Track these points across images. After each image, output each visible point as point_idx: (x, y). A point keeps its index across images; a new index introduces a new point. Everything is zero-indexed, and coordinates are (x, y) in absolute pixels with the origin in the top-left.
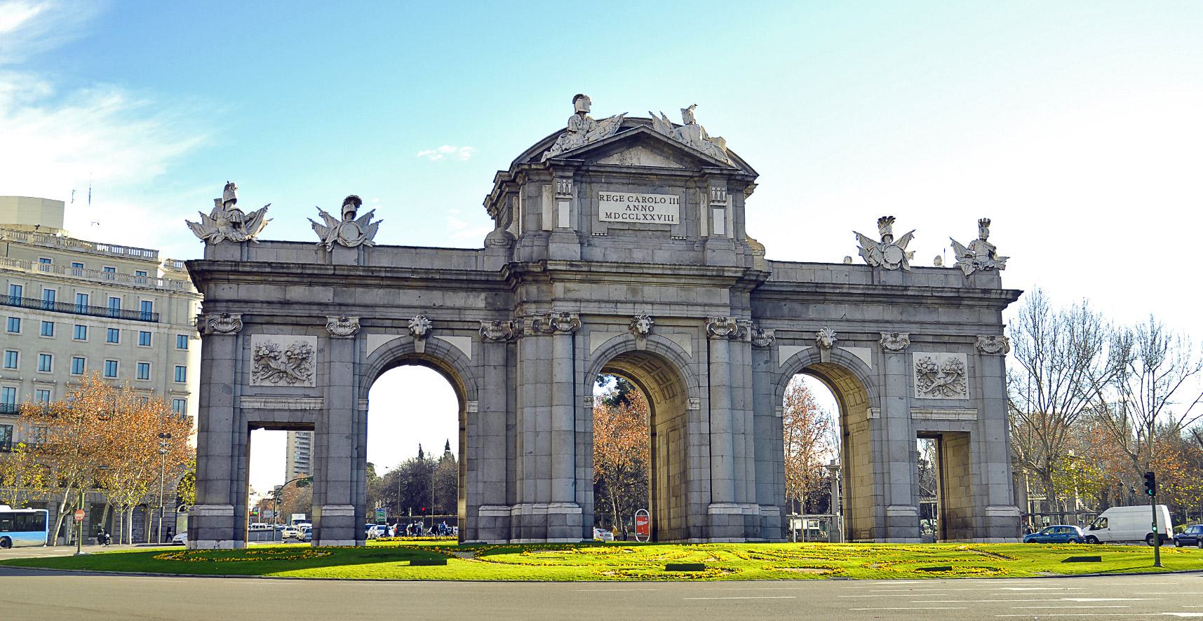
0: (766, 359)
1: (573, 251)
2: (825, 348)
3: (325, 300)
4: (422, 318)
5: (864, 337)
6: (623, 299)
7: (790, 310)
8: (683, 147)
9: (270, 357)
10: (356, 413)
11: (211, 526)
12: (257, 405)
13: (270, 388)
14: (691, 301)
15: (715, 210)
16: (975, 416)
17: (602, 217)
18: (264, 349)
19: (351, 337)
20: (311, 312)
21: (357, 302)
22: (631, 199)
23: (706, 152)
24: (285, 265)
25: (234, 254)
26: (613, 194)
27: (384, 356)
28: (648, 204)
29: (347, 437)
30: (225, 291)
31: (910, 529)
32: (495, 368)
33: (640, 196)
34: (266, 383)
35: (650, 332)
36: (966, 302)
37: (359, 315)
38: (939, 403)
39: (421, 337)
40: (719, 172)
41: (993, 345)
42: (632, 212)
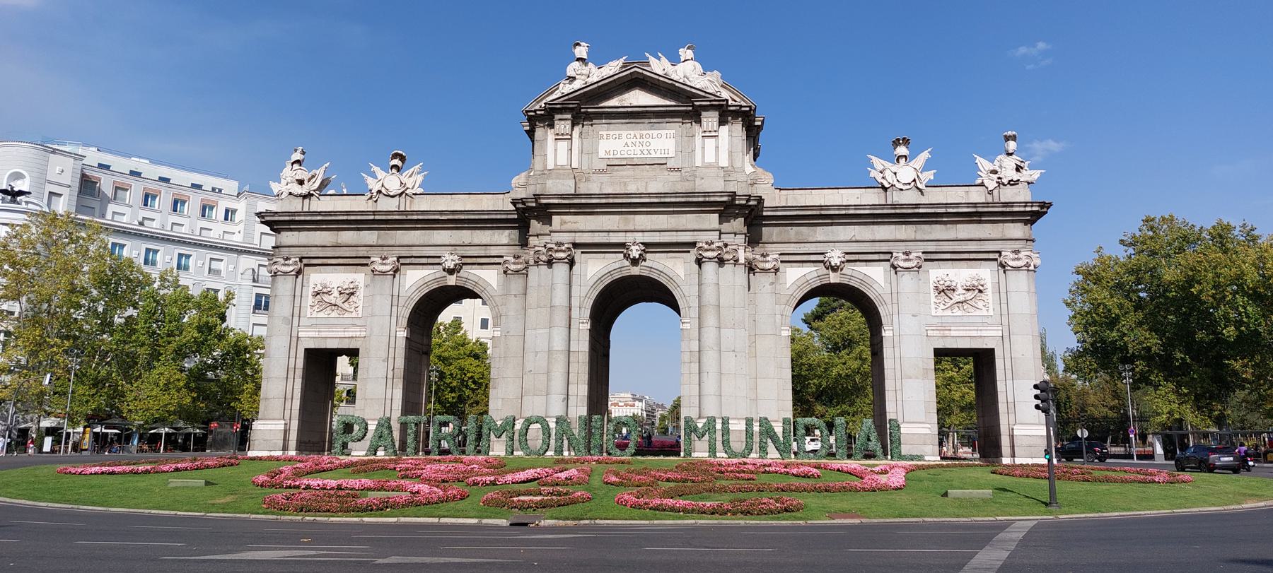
0: (771, 281)
1: (567, 187)
2: (835, 269)
3: (371, 243)
4: (452, 254)
5: (876, 257)
6: (615, 228)
7: (797, 233)
8: (674, 83)
9: (323, 293)
10: (393, 339)
11: (265, 438)
14: (681, 228)
15: (707, 140)
16: (1001, 332)
17: (602, 155)
18: (319, 285)
19: (391, 273)
21: (398, 244)
22: (629, 136)
23: (697, 87)
25: (296, 205)
26: (611, 133)
27: (420, 289)
28: (645, 140)
29: (384, 361)
30: (289, 237)
31: (923, 447)
32: (516, 297)
33: (638, 133)
35: (642, 258)
38: (958, 320)
39: (451, 272)
40: (708, 103)
41: (1018, 259)
42: (630, 148)
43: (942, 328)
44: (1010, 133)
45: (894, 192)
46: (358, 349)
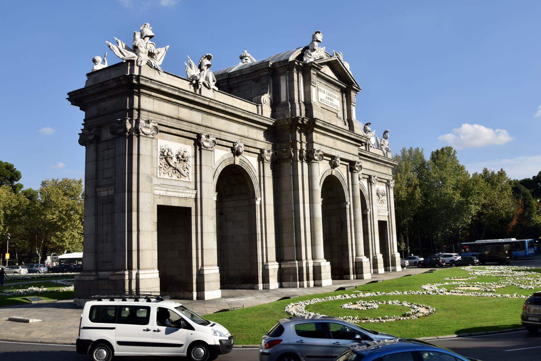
3: (198, 122)
12: (162, 193)
18: (167, 151)
20: (192, 128)
21: (213, 126)
24: (187, 93)
26: (322, 89)
28: (331, 97)
32: (268, 178)
34: (166, 176)
37: (214, 135)
40: (355, 88)
43: (378, 210)
45: (370, 148)
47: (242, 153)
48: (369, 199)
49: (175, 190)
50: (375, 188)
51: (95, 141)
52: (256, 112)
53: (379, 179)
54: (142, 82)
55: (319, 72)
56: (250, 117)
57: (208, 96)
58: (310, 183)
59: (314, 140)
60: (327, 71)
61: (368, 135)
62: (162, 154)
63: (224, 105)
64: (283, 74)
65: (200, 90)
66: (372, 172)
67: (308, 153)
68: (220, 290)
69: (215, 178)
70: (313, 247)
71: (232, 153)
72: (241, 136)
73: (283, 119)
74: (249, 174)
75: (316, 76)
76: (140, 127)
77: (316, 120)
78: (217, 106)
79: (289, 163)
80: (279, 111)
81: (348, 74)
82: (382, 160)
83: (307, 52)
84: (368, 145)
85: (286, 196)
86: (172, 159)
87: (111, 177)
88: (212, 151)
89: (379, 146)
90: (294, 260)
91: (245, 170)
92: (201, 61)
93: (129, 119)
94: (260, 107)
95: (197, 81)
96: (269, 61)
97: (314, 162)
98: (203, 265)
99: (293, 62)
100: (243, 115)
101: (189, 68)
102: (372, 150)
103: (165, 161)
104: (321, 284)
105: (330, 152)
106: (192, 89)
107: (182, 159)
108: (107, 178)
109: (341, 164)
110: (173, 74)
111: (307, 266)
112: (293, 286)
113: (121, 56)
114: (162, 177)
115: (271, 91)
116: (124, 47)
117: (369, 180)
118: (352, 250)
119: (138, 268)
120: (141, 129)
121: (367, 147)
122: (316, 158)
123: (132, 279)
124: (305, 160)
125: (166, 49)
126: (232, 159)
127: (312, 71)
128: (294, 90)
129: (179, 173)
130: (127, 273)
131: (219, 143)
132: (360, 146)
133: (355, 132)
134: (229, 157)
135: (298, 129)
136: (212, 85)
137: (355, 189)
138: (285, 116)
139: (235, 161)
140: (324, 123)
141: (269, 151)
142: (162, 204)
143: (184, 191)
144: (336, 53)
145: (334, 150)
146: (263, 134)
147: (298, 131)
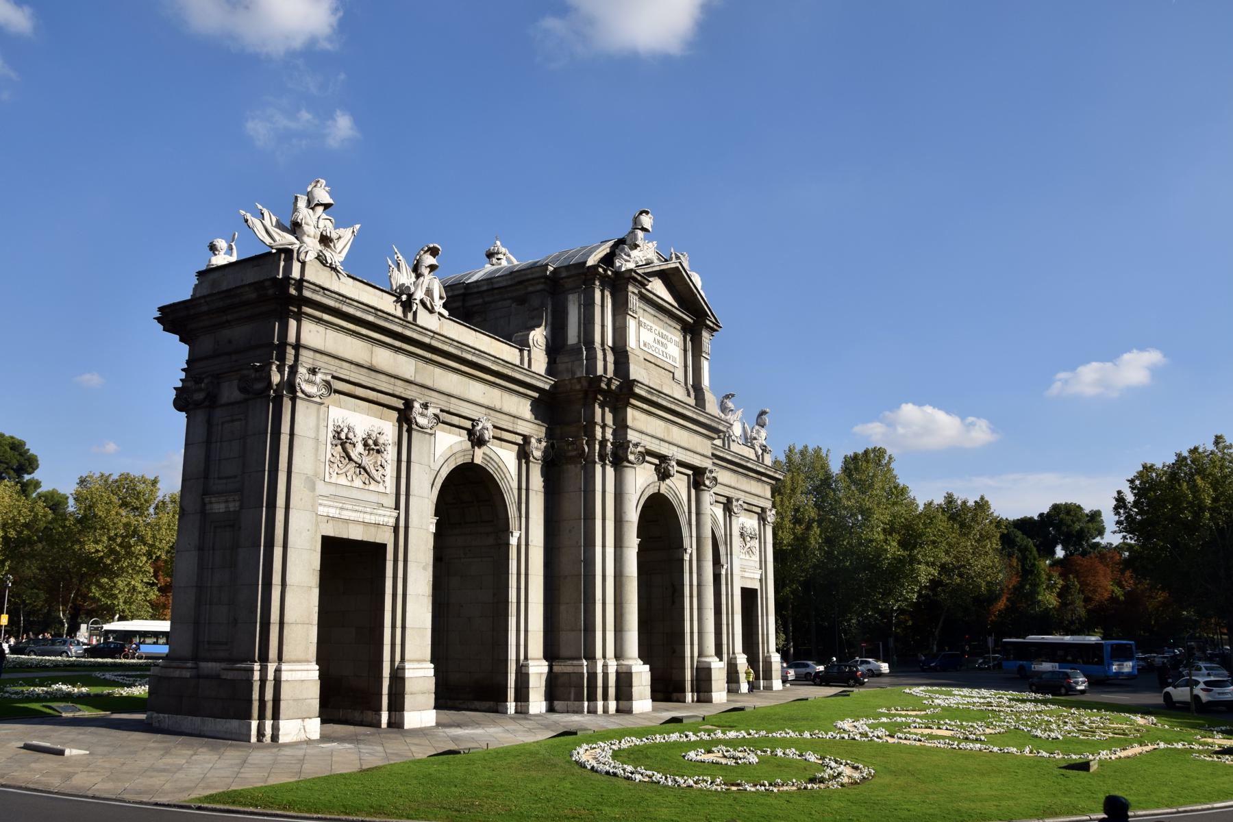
3: (407, 376)
12: (333, 512)
13: (344, 488)
18: (346, 430)
20: (396, 388)
21: (436, 387)
24: (391, 318)
26: (648, 323)
28: (663, 340)
36: (763, 478)
40: (711, 324)
44: (768, 410)
45: (731, 443)
46: (386, 545)
47: (488, 442)
48: (726, 544)
49: (357, 508)
50: (737, 524)
51: (207, 403)
52: (518, 363)
53: (745, 506)
54: (307, 293)
55: (643, 291)
56: (508, 371)
57: (429, 327)
58: (618, 506)
59: (629, 423)
60: (658, 288)
61: (728, 417)
62: (336, 435)
63: (460, 345)
64: (573, 290)
65: (415, 314)
66: (733, 490)
67: (616, 448)
68: (435, 710)
69: (434, 487)
70: (617, 633)
71: (469, 440)
72: (488, 408)
73: (570, 379)
74: (500, 484)
75: (637, 298)
76: (298, 380)
77: (636, 383)
78: (446, 348)
79: (579, 466)
80: (564, 362)
81: (698, 296)
82: (754, 467)
83: (623, 250)
84: (728, 438)
85: (570, 531)
86: (354, 446)
87: (235, 477)
88: (431, 434)
89: (749, 441)
90: (580, 659)
91: (492, 475)
92: (418, 257)
93: (278, 363)
94: (526, 353)
95: (410, 296)
96: (547, 265)
97: (627, 467)
98: (403, 659)
99: (595, 267)
100: (495, 367)
101: (396, 269)
102: (735, 447)
103: (341, 451)
104: (631, 708)
105: (658, 447)
106: (399, 312)
107: (373, 447)
108: (227, 478)
109: (677, 472)
110: (365, 281)
111: (605, 671)
112: (576, 709)
113: (268, 240)
114: (333, 480)
115: (549, 322)
116: (274, 224)
117: (728, 507)
118: (692, 644)
119: (280, 659)
120: (299, 384)
121: (726, 442)
122: (631, 457)
123: (267, 680)
124: (609, 461)
125: (353, 232)
126: (468, 453)
127: (631, 288)
128: (594, 324)
129: (366, 475)
130: (257, 666)
131: (446, 420)
132: (714, 439)
133: (707, 411)
134: (464, 448)
135: (599, 400)
136: (438, 305)
137: (702, 523)
138: (573, 373)
139: (473, 456)
140: (649, 389)
141: (539, 441)
142: (331, 534)
143: (375, 511)
144: (676, 254)
145: (667, 444)
146: (531, 405)
147: (599, 404)
